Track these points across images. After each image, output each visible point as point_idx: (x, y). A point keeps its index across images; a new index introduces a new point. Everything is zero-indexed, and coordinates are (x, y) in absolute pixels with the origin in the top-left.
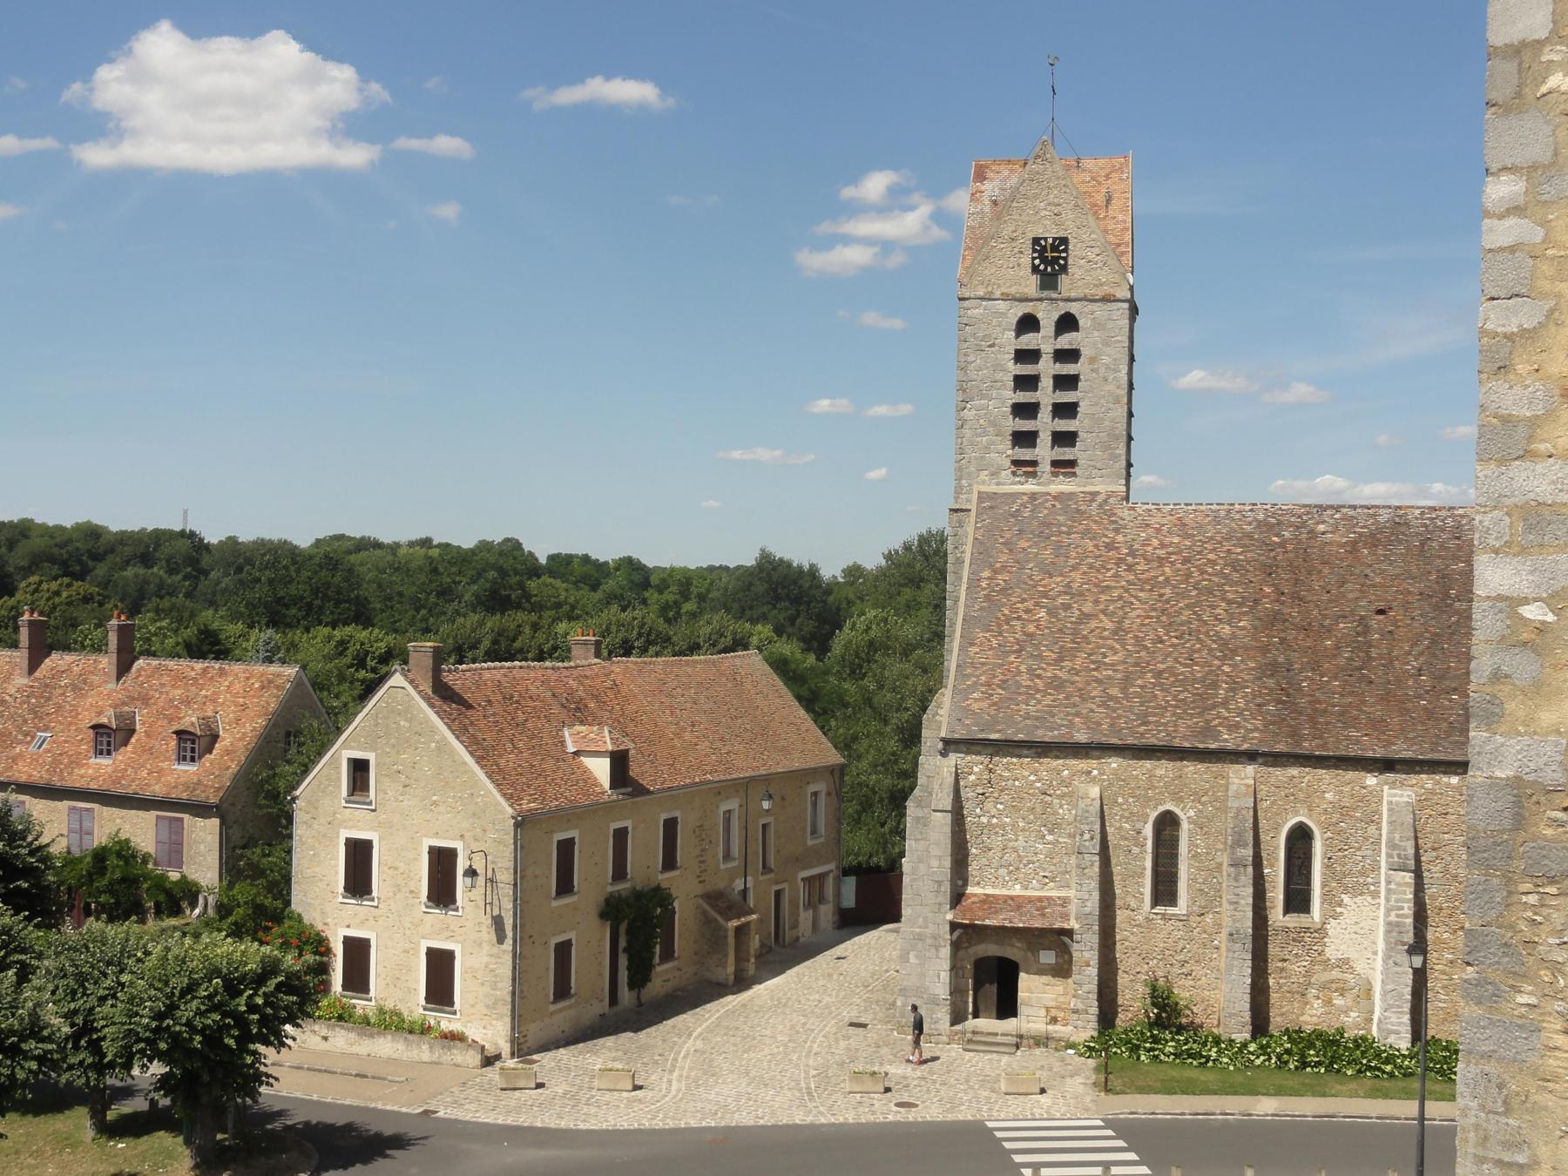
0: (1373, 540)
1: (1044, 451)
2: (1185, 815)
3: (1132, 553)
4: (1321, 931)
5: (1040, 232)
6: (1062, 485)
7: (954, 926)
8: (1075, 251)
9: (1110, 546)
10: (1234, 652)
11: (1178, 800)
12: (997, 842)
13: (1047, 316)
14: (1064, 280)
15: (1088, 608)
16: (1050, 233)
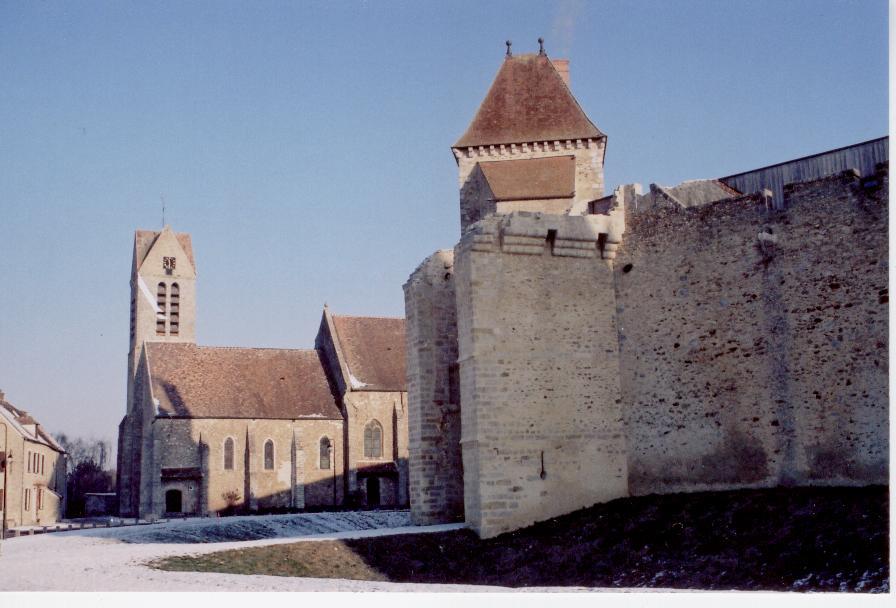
0: (276, 358)
1: (168, 327)
2: (234, 438)
3: (202, 362)
4: (276, 473)
5: (167, 255)
6: (174, 339)
7: (162, 478)
8: (178, 263)
9: (195, 360)
10: (242, 391)
11: (232, 433)
12: (174, 451)
13: (169, 282)
14: (174, 272)
15: (192, 378)
16: (170, 255)
